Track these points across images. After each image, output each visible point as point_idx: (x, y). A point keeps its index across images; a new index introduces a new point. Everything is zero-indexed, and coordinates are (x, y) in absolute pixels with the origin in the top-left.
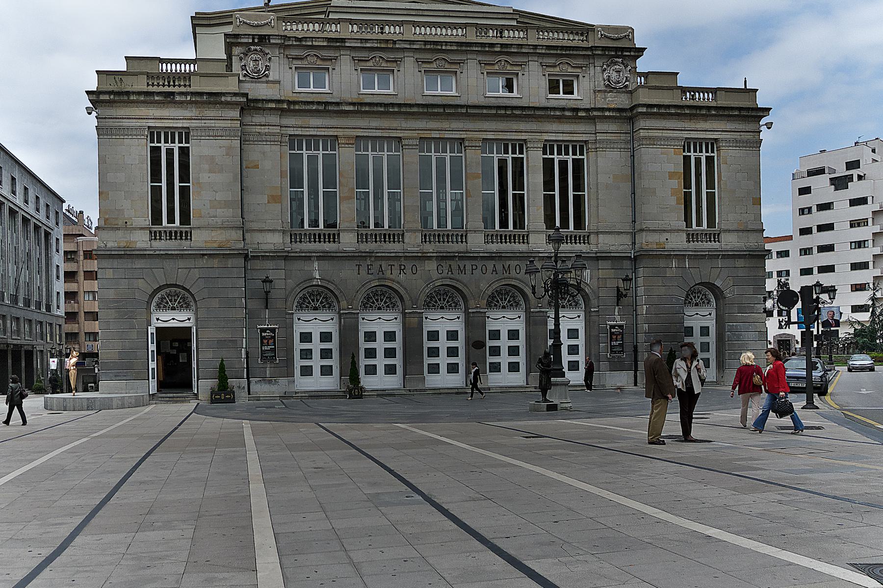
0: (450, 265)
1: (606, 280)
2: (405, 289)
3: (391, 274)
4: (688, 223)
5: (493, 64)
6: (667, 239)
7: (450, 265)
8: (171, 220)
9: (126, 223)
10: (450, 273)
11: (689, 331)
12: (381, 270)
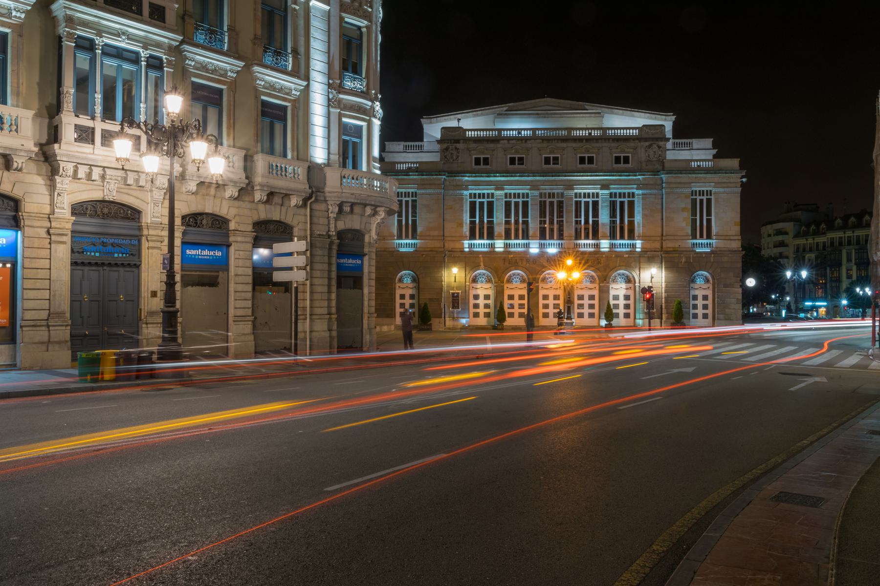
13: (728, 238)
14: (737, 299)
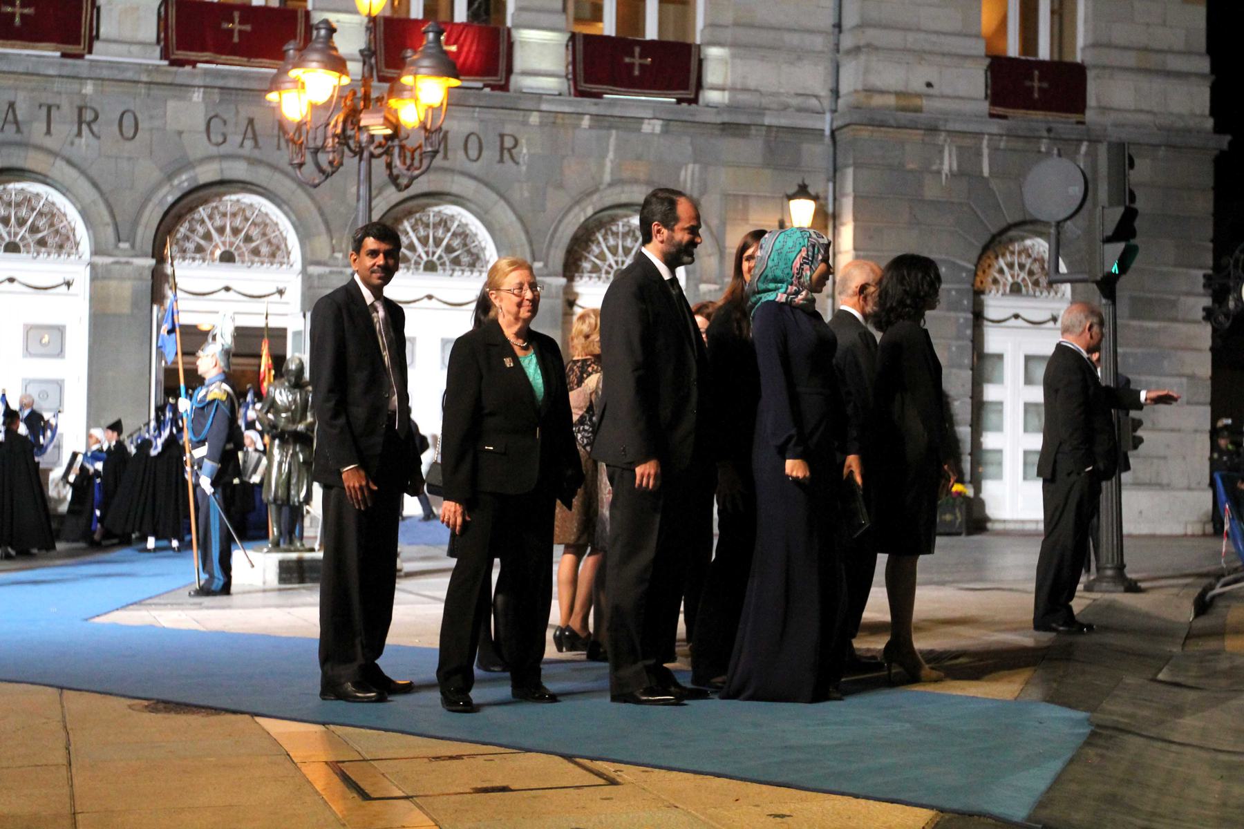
3: (48, 132)
7: (251, 122)
10: (249, 144)
12: (10, 117)
13: (1154, 61)
14: (1192, 377)
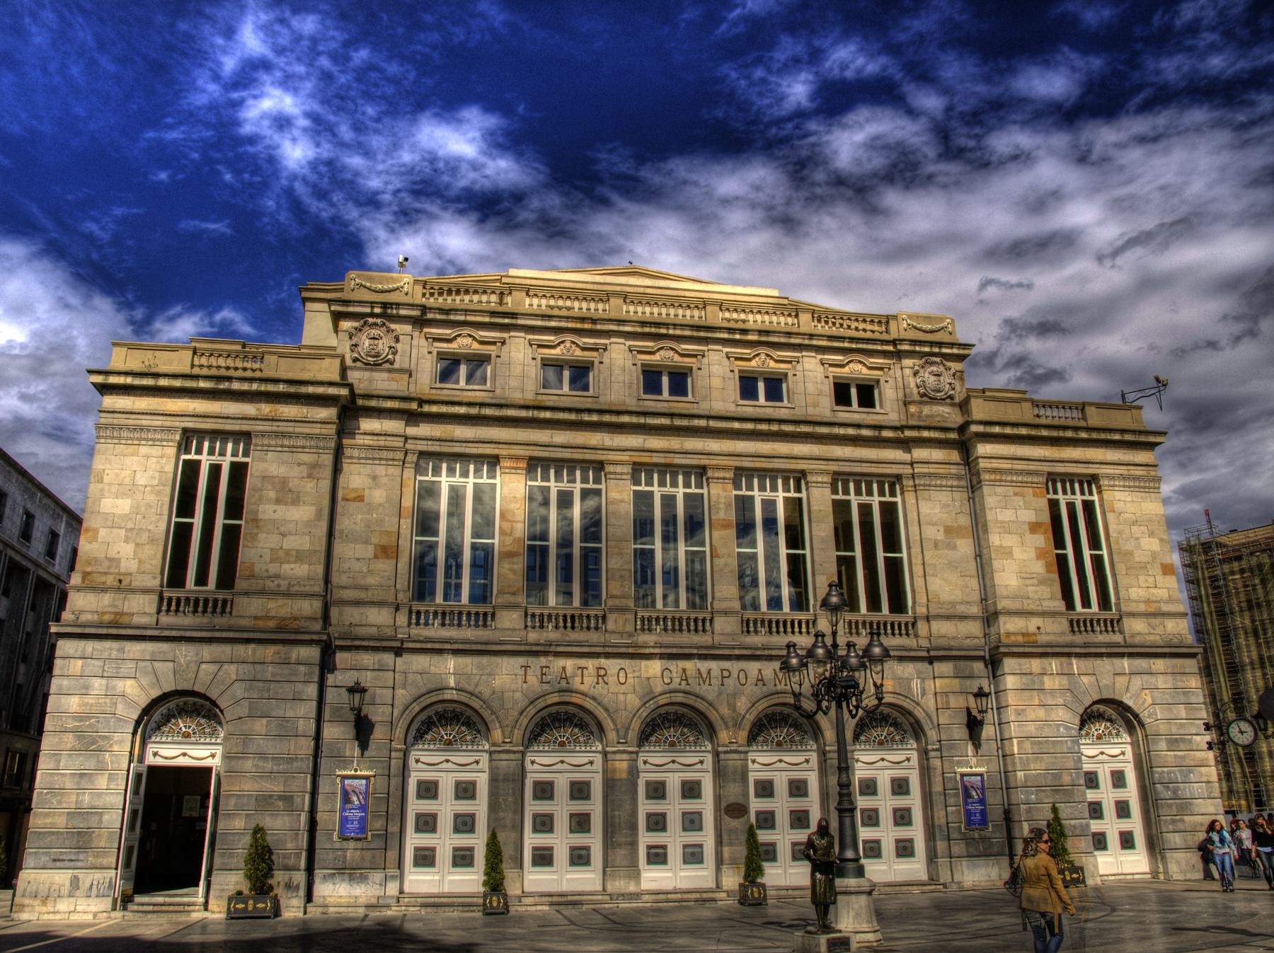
0: (684, 670)
1: (947, 696)
2: (606, 710)
3: (582, 683)
4: (1070, 605)
5: (749, 360)
6: (1039, 628)
7: (684, 670)
8: (202, 579)
9: (120, 581)
11: (1092, 780)
